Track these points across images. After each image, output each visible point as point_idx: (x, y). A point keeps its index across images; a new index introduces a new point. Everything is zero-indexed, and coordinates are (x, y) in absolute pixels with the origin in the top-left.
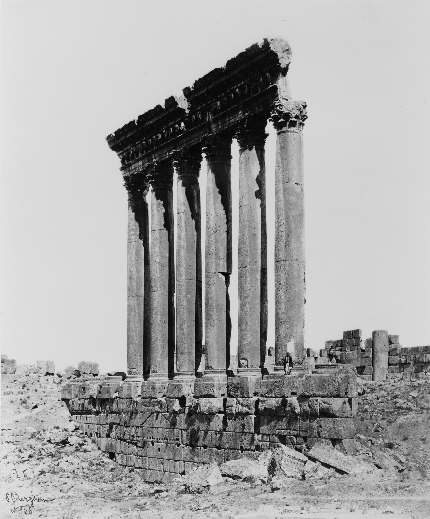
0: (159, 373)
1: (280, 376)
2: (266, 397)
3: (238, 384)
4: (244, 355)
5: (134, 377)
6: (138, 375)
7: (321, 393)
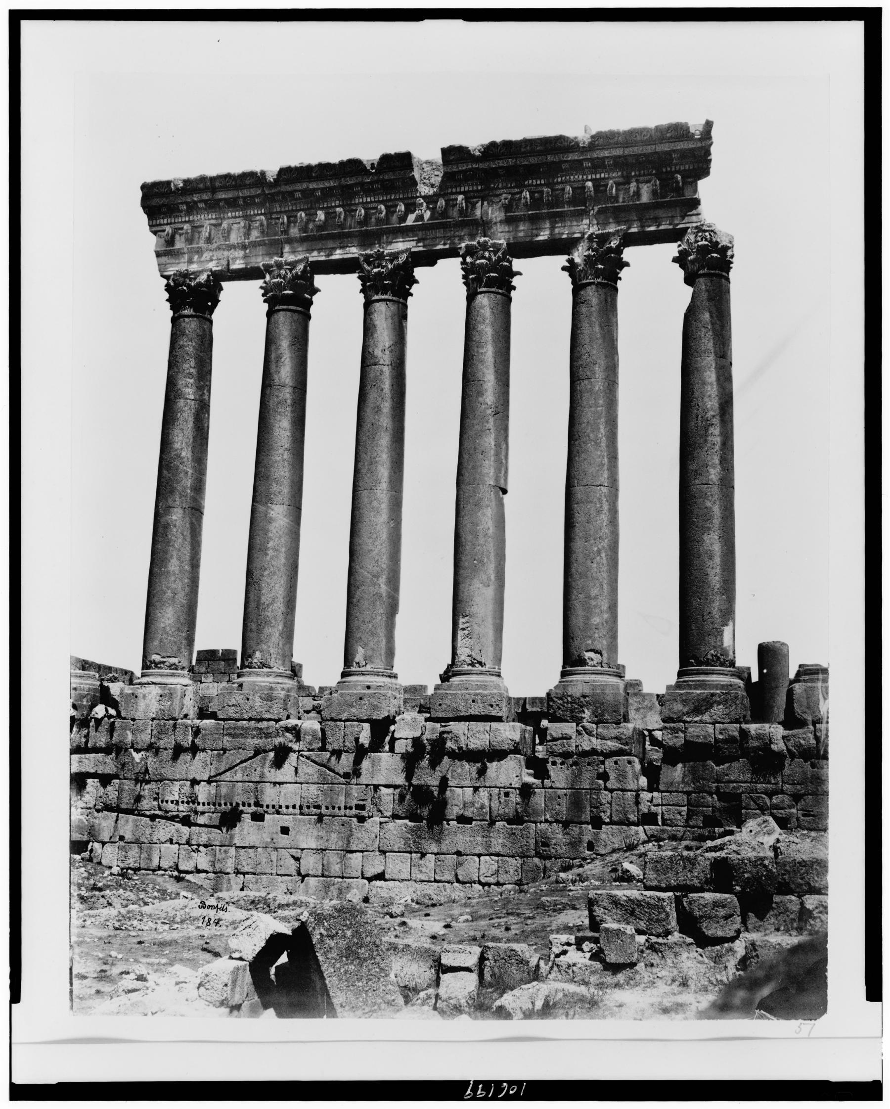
0: (275, 669)
1: (723, 686)
3: (584, 696)
4: (596, 643)
5: (173, 675)
6: (180, 671)
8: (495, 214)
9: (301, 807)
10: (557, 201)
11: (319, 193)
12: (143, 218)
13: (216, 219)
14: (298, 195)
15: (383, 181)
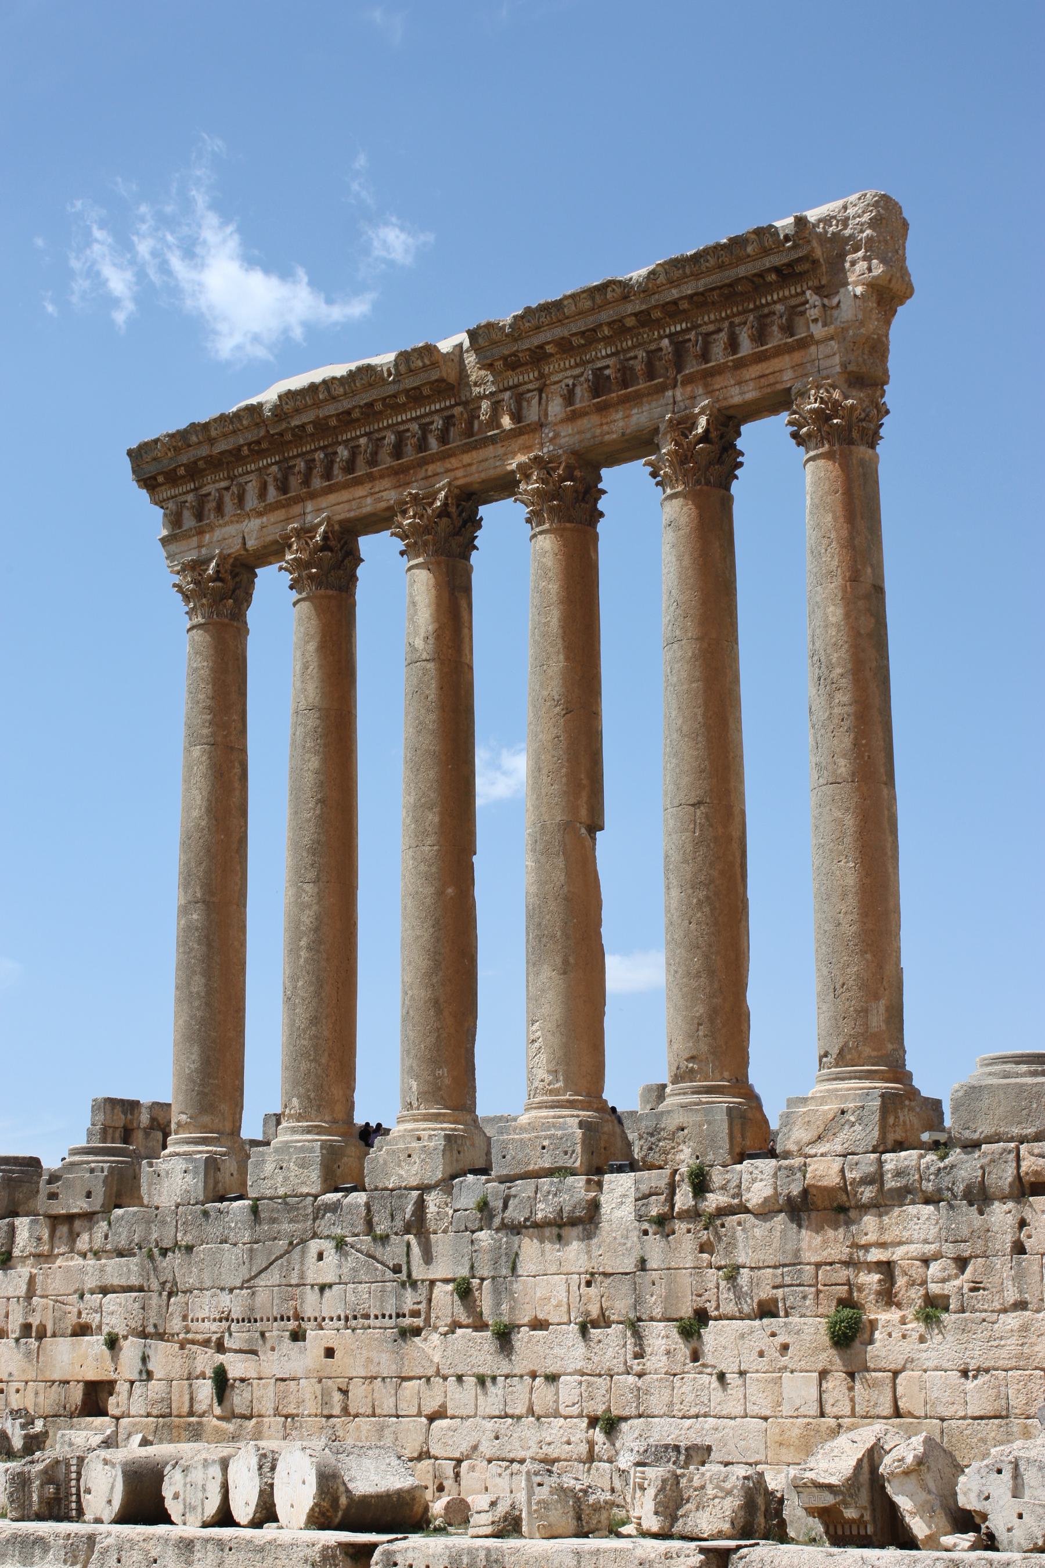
2: (807, 1156)
7: (1016, 1131)
8: (556, 408)
9: (347, 1319)
11: (333, 422)
12: (144, 494)
13: (225, 479)
14: (310, 429)
15: (407, 392)
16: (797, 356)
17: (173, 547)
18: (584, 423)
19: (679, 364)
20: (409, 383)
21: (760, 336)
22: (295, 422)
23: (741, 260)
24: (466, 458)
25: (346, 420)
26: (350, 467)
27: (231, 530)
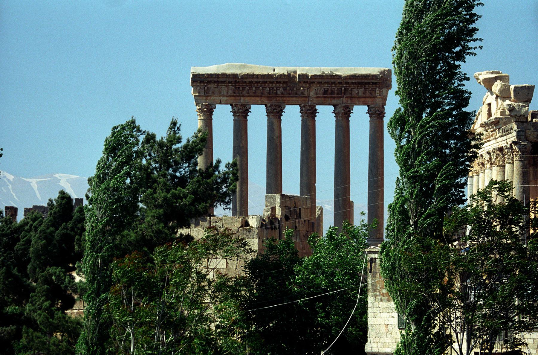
8: (312, 93)
10: (332, 93)
16: (373, 99)
17: (197, 98)
18: (320, 99)
19: (345, 94)
20: (279, 80)
21: (364, 93)
22: (245, 80)
23: (367, 79)
24: (288, 99)
25: (257, 82)
26: (255, 93)
27: (217, 98)
